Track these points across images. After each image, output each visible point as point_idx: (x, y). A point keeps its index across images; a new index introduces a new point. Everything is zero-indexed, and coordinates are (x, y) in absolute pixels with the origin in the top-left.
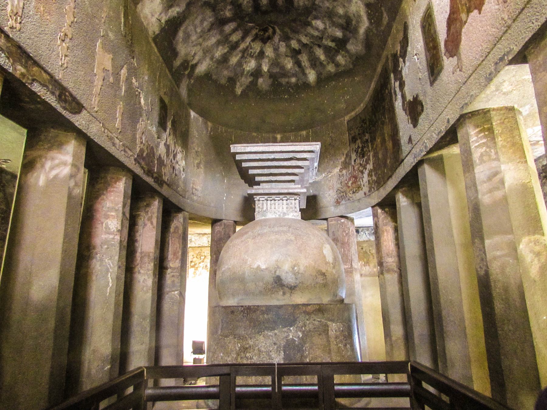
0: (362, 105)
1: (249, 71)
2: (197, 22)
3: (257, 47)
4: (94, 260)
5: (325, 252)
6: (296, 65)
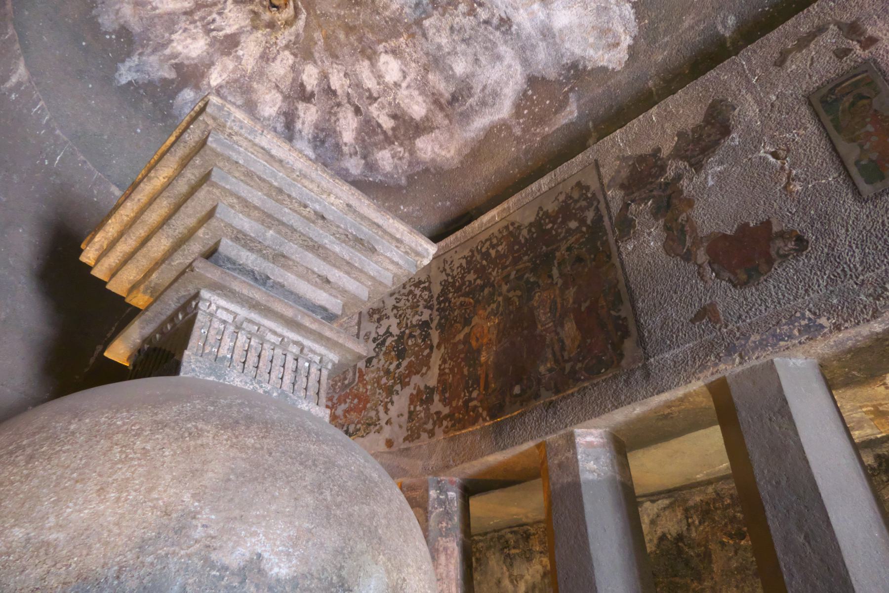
1: (175, 56)
6: (282, 119)
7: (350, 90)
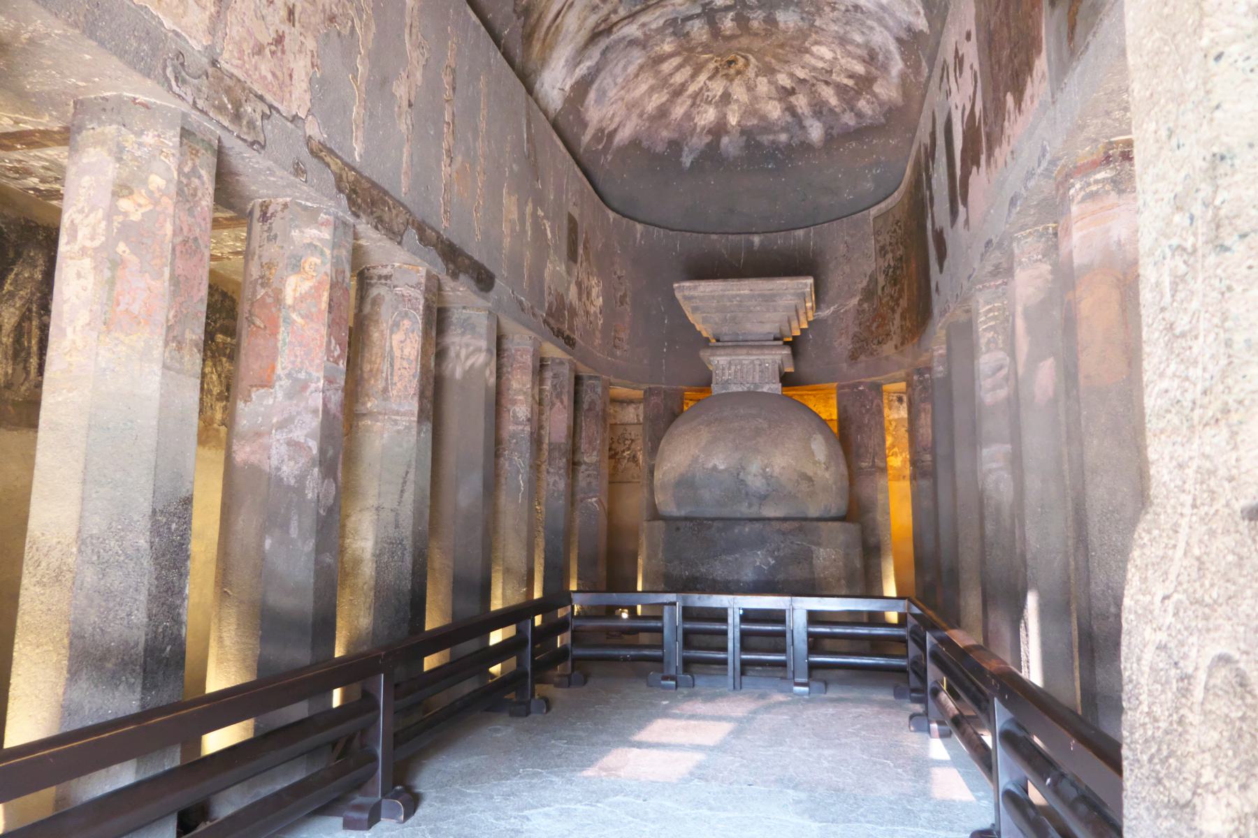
2: (618, 70)
3: (718, 87)
6: (787, 113)
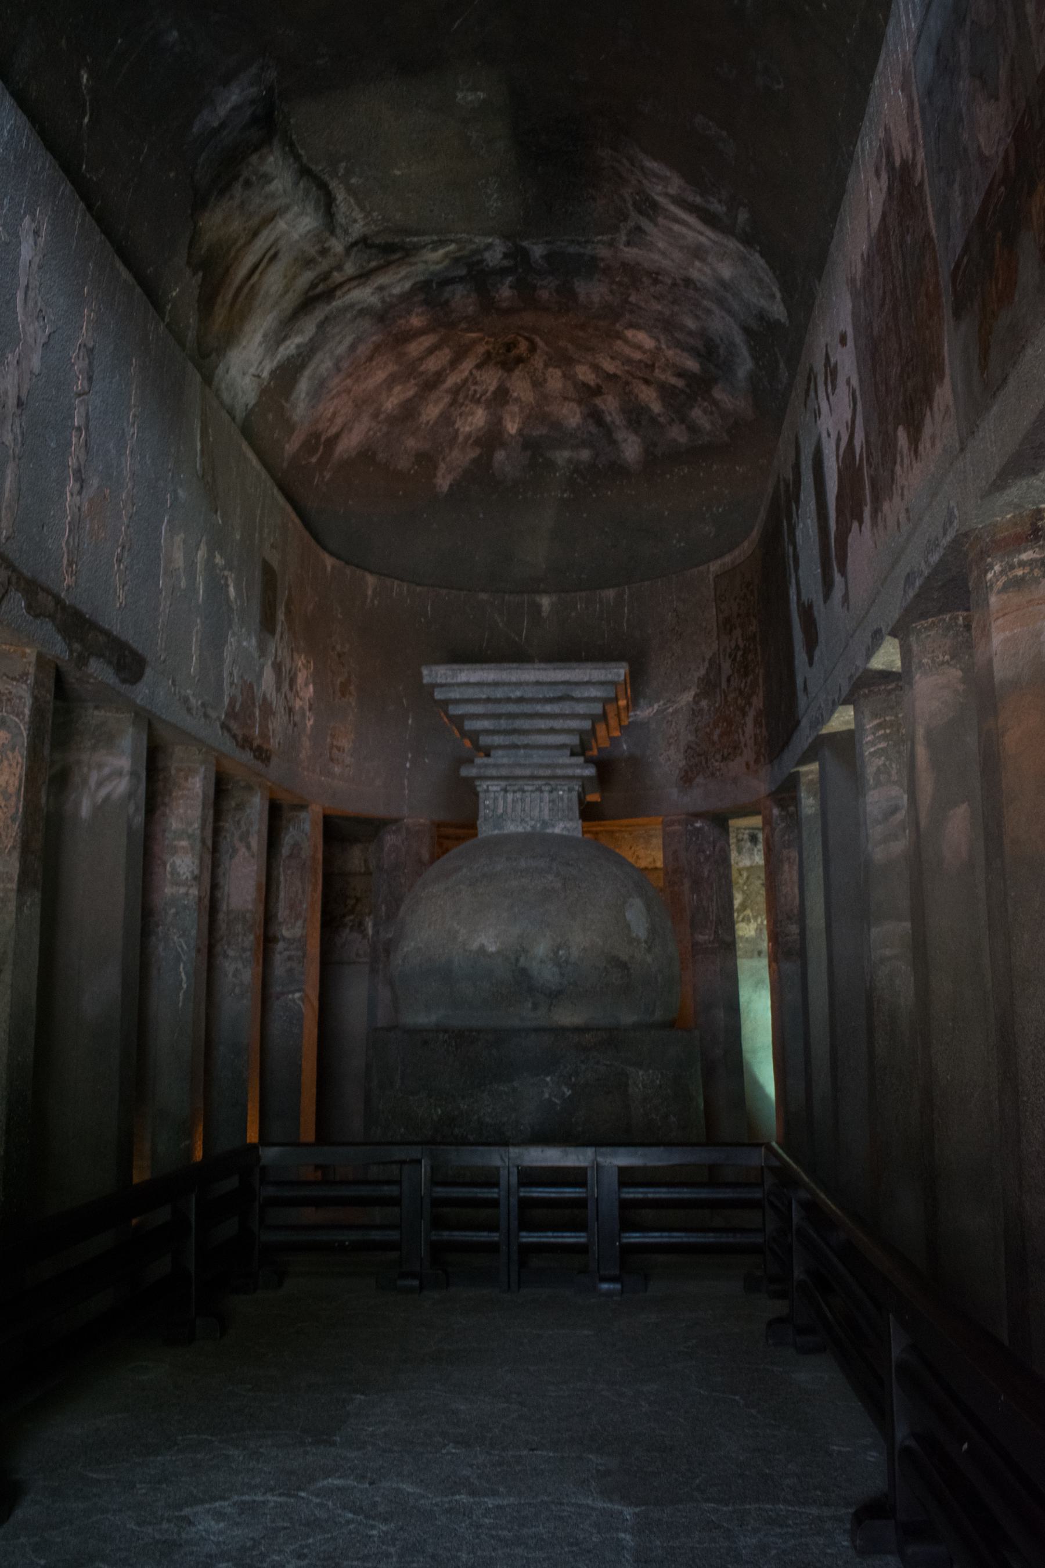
0: (746, 544)
1: (468, 436)
3: (490, 379)
4: (154, 938)
5: (629, 915)
6: (590, 421)
7: (626, 368)
